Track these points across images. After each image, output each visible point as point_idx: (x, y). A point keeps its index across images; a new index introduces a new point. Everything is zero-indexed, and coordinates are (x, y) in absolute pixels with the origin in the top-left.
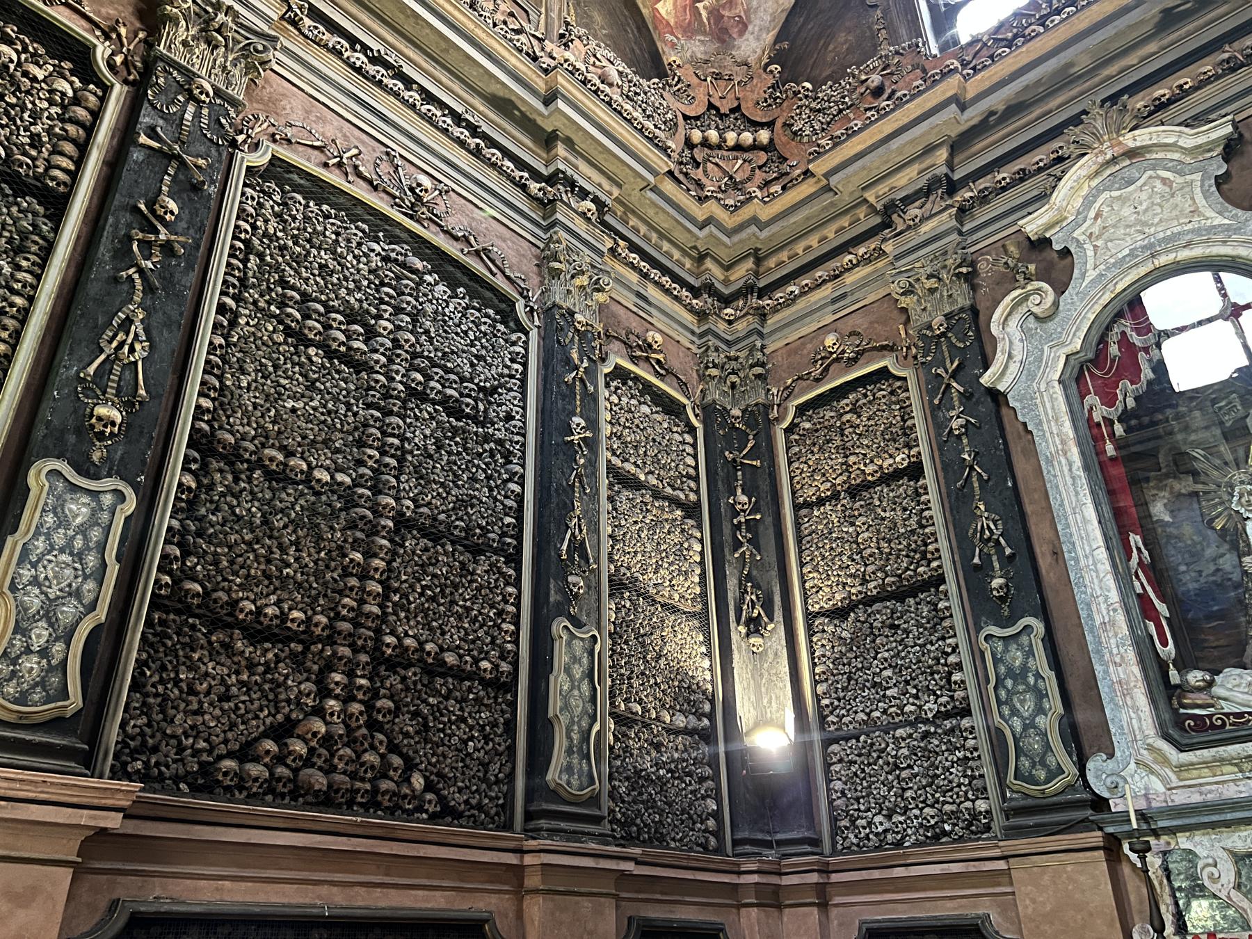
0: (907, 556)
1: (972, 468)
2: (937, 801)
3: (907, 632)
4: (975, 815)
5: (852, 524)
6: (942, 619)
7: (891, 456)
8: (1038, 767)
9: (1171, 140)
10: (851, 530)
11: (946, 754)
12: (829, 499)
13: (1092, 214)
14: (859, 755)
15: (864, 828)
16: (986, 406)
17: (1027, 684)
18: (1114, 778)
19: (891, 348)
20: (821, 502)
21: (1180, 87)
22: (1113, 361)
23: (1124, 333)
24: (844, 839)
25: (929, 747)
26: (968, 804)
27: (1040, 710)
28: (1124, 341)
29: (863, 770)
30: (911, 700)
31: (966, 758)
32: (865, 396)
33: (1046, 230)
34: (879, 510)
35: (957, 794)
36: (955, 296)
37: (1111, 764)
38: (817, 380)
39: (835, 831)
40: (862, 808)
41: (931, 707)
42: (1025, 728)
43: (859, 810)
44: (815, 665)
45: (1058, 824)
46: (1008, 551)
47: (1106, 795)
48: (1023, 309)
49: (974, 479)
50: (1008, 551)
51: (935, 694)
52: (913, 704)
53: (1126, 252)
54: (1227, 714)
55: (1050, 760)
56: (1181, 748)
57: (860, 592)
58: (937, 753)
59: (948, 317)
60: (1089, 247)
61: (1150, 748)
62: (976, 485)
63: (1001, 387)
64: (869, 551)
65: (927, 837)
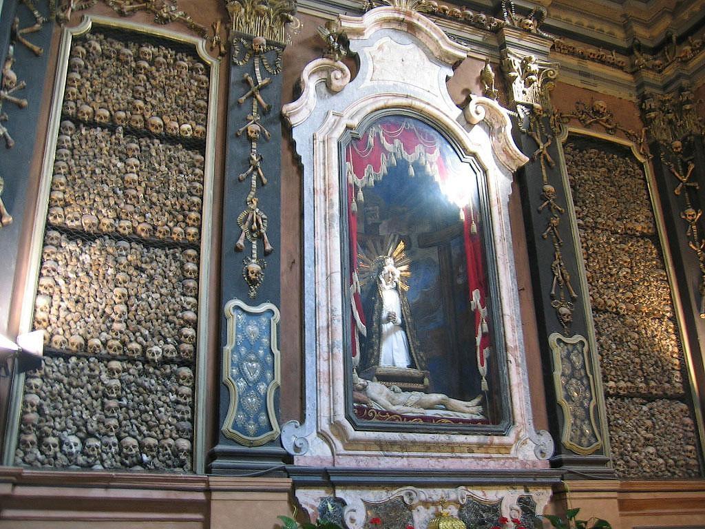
0: (170, 213)
1: (255, 169)
2: (141, 432)
3: (151, 278)
4: (176, 452)
5: (121, 160)
6: (186, 278)
7: (178, 121)
8: (252, 422)
9: (436, 37)
10: (120, 165)
11: (160, 394)
12: (103, 127)
13: (377, 45)
14: (68, 375)
15: (55, 446)
16: (278, 128)
17: (257, 355)
18: (302, 441)
19: (201, 33)
20: (92, 124)
21: (445, 10)
22: (369, 149)
23: (378, 134)
24: (26, 453)
25: (146, 384)
26: (171, 441)
27: (262, 378)
28: (377, 138)
29: (69, 392)
30: (140, 339)
31: (178, 402)
32: (165, 57)
33: (350, 33)
34: (154, 160)
35: (162, 432)
36: (275, 30)
37: (299, 432)
38: (121, 14)
39: (21, 444)
40: (58, 426)
41: (157, 349)
42: (248, 388)
43: (54, 428)
44: (41, 275)
45: (259, 469)
46: (268, 247)
47: (292, 452)
48: (324, 75)
49: (254, 177)
50: (268, 247)
51: (165, 338)
52: (140, 343)
53: (391, 83)
54: (377, 411)
55: (263, 418)
56: (356, 428)
57: (112, 225)
58: (151, 391)
59: (268, 43)
60: (370, 62)
61: (336, 425)
62: (254, 182)
63: (293, 121)
64: (134, 192)
65: (123, 463)
